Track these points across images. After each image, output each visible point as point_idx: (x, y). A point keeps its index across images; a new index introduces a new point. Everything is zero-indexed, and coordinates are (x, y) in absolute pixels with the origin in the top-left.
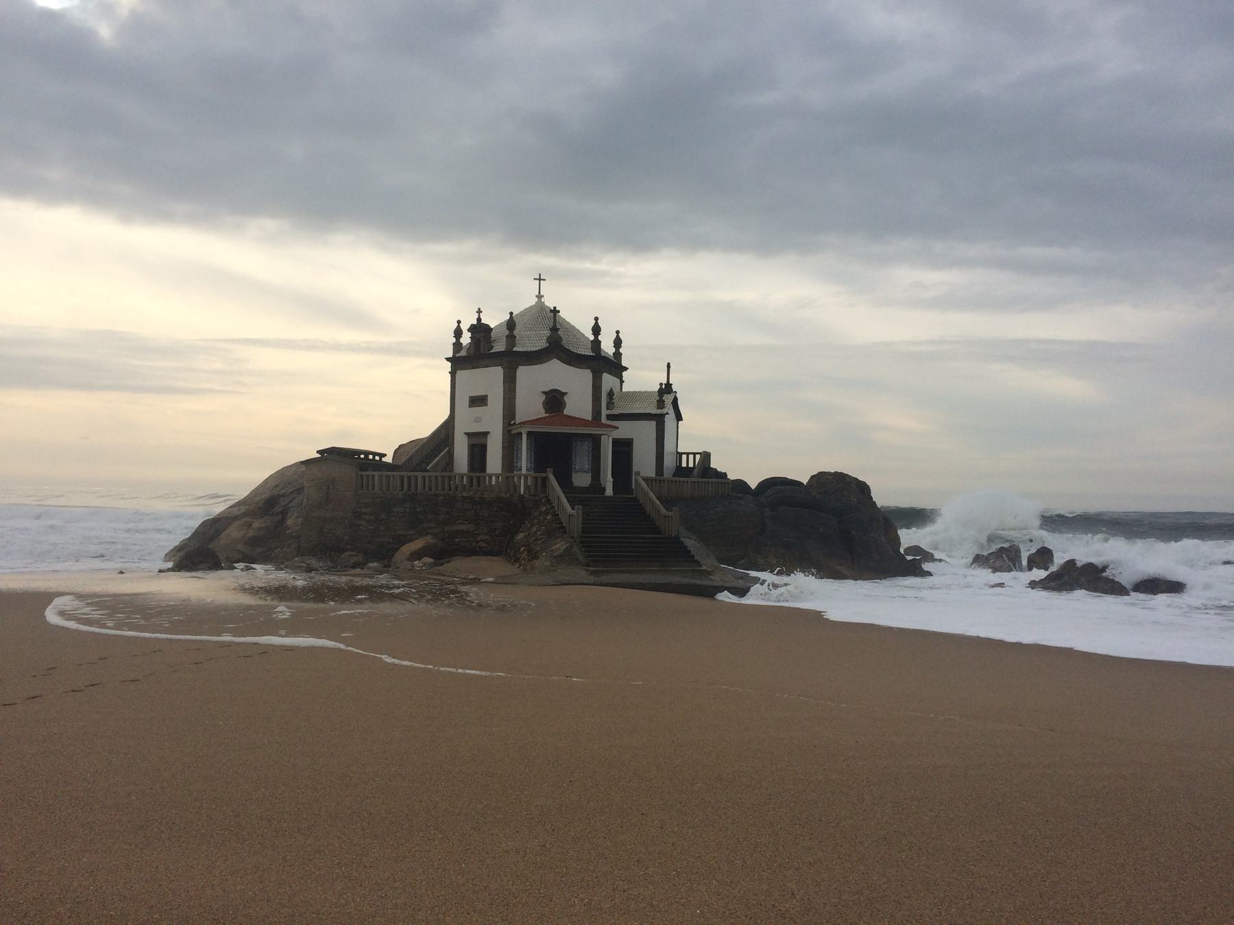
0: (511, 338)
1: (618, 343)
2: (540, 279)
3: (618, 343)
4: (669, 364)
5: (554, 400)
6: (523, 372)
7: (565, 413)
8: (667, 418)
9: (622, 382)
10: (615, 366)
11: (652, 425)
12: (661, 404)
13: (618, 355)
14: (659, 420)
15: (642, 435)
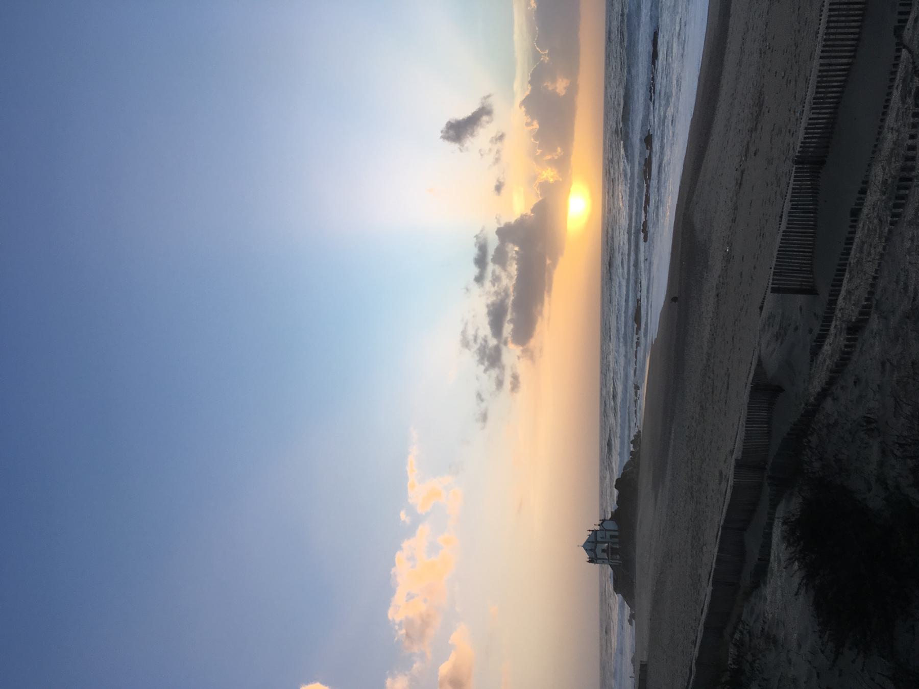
0: (592, 558)
1: (590, 531)
2: (578, 546)
3: (590, 531)
4: (595, 525)
5: (603, 551)
6: (598, 557)
7: (606, 548)
8: (606, 529)
9: (597, 530)
10: (595, 532)
11: (607, 532)
12: (603, 530)
13: (592, 531)
14: (606, 530)
15: (608, 534)
